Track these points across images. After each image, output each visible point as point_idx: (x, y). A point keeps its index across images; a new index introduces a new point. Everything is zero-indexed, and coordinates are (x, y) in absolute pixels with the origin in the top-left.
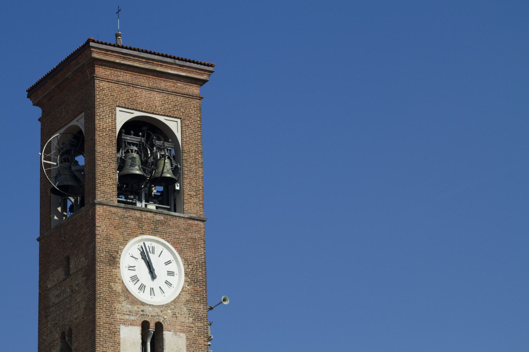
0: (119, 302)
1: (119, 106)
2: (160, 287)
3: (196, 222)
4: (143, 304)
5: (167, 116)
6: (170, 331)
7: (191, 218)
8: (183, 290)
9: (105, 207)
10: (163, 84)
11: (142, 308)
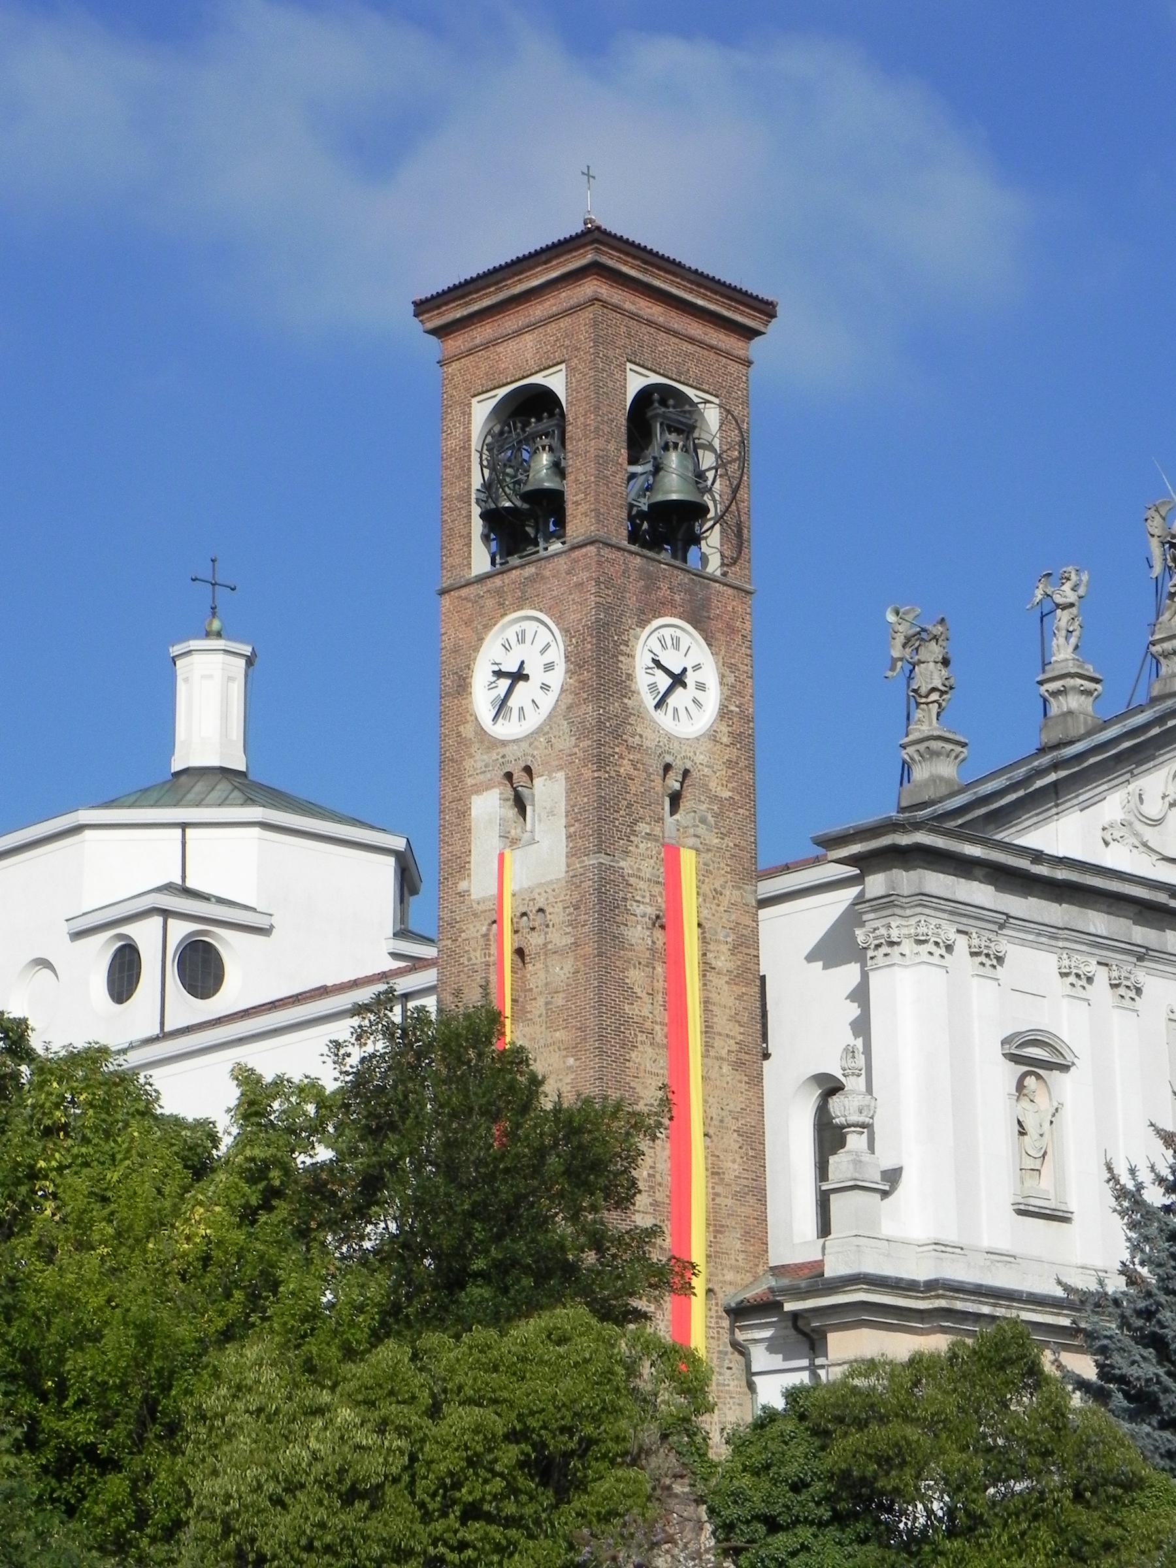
0: (471, 756)
1: (475, 396)
3: (584, 550)
4: (504, 743)
5: (545, 369)
7: (574, 548)
8: (562, 691)
11: (502, 751)
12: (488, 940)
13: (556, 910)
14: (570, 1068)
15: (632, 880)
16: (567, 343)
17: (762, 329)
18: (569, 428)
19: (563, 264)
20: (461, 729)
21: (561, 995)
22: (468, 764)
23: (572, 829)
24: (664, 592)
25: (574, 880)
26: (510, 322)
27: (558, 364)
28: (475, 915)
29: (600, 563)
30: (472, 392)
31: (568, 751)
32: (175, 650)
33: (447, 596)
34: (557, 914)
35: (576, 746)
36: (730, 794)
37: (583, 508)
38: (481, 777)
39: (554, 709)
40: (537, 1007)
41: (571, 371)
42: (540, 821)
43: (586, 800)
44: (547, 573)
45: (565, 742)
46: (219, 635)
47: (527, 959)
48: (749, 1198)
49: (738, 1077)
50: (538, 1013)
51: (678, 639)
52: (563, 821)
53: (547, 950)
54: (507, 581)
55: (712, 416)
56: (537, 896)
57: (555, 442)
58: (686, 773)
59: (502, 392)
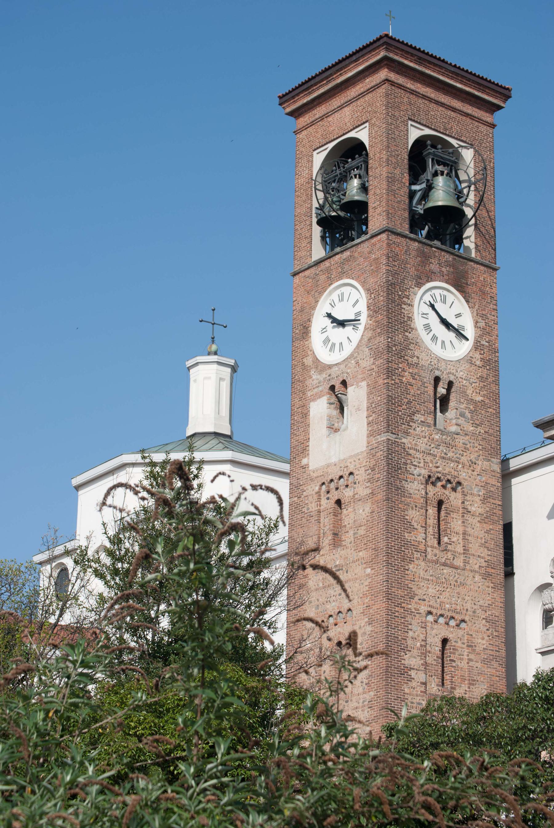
2: (348, 338)
3: (379, 237)
4: (330, 367)
5: (357, 127)
6: (353, 385)
7: (373, 237)
9: (300, 274)
10: (353, 92)
11: (329, 372)
12: (320, 495)
13: (361, 472)
14: (368, 575)
15: (411, 452)
16: (370, 109)
17: (502, 105)
18: (370, 162)
19: (367, 60)
20: (305, 360)
21: (363, 528)
22: (309, 382)
23: (371, 419)
24: (434, 266)
25: (371, 451)
26: (336, 102)
27: (364, 123)
28: (312, 480)
29: (389, 245)
30: (314, 147)
31: (368, 368)
32: (189, 363)
33: (297, 277)
34: (361, 475)
35: (374, 364)
36: (481, 398)
37: (379, 210)
38: (316, 390)
39: (360, 341)
40: (348, 538)
41: (372, 126)
42: (351, 415)
43: (379, 398)
44: (356, 255)
45: (367, 362)
46: (216, 353)
47: (343, 506)
48: (493, 663)
49: (487, 584)
50: (349, 541)
51: (445, 297)
52: (365, 414)
53: (355, 499)
54: (332, 263)
55: (468, 155)
56: (349, 464)
57: (362, 172)
58: (450, 384)
59: (331, 146)
